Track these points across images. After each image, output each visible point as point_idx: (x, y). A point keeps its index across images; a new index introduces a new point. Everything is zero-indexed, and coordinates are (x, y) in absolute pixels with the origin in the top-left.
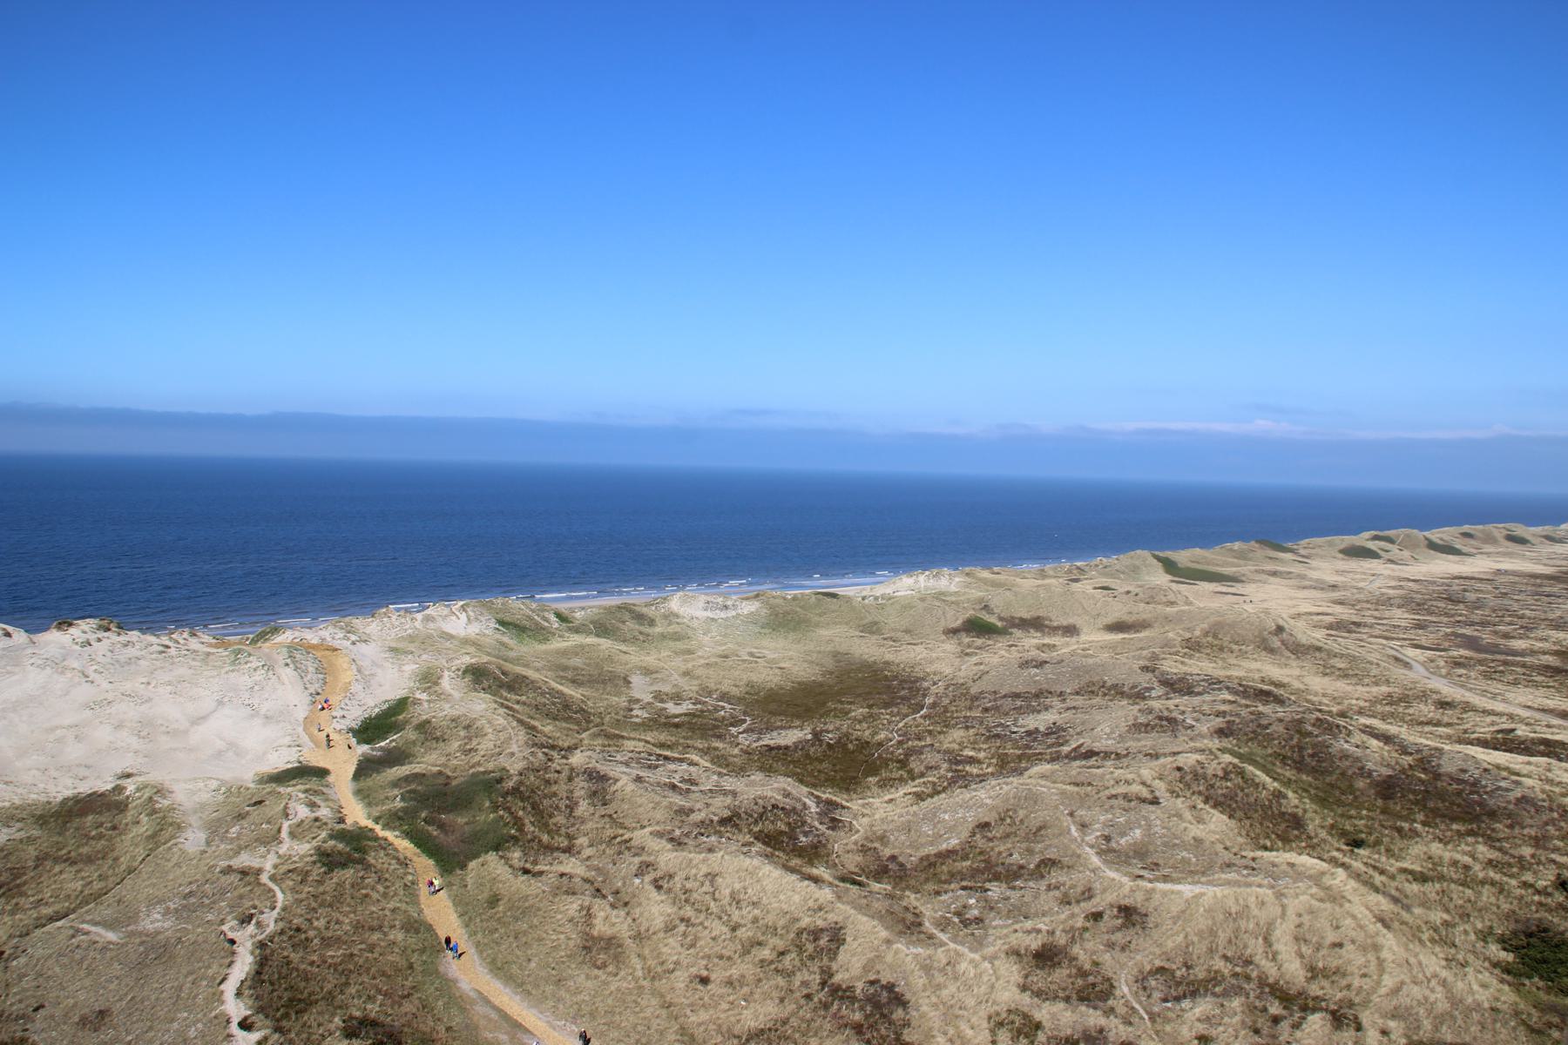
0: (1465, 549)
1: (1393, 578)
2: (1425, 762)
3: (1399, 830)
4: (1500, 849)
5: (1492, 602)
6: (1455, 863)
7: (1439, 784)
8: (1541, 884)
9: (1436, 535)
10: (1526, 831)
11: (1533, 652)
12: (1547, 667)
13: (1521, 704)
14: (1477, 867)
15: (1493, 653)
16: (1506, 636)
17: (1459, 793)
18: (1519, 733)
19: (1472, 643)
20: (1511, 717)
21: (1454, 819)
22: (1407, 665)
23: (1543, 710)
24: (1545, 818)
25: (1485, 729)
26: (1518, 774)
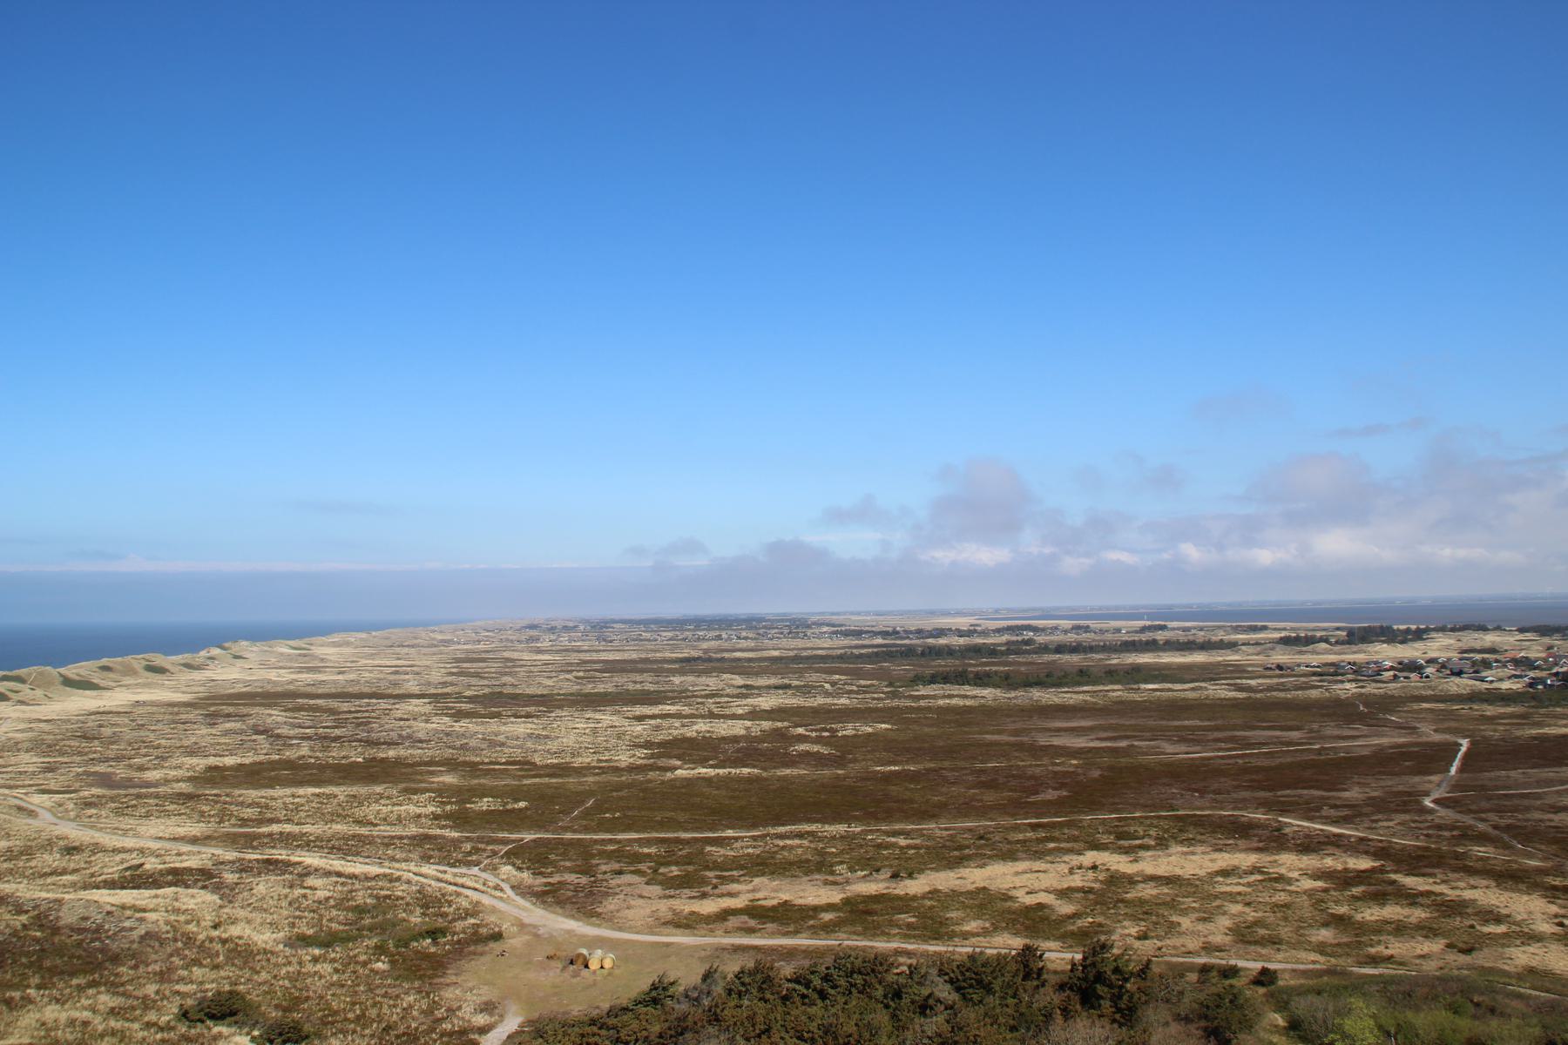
0: (103, 683)
1: (23, 720)
2: (43, 918)
3: (9, 1003)
4: (124, 994)
5: (129, 735)
6: (72, 1022)
7: (56, 939)
8: (165, 1019)
9: (71, 671)
10: (150, 969)
11: (167, 781)
12: (180, 795)
13: (156, 837)
14: (97, 1020)
15: (126, 787)
16: (141, 768)
17: (79, 944)
18: (147, 867)
19: (105, 780)
20: (142, 851)
21: (73, 974)
22: (31, 814)
23: (175, 839)
24: (169, 950)
25: (112, 868)
26: (144, 910)
